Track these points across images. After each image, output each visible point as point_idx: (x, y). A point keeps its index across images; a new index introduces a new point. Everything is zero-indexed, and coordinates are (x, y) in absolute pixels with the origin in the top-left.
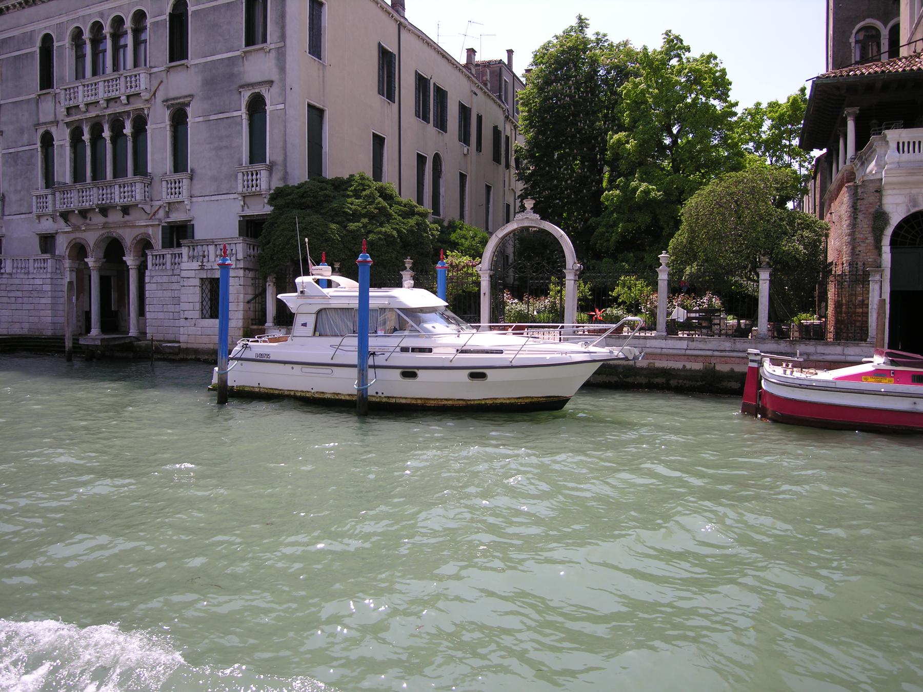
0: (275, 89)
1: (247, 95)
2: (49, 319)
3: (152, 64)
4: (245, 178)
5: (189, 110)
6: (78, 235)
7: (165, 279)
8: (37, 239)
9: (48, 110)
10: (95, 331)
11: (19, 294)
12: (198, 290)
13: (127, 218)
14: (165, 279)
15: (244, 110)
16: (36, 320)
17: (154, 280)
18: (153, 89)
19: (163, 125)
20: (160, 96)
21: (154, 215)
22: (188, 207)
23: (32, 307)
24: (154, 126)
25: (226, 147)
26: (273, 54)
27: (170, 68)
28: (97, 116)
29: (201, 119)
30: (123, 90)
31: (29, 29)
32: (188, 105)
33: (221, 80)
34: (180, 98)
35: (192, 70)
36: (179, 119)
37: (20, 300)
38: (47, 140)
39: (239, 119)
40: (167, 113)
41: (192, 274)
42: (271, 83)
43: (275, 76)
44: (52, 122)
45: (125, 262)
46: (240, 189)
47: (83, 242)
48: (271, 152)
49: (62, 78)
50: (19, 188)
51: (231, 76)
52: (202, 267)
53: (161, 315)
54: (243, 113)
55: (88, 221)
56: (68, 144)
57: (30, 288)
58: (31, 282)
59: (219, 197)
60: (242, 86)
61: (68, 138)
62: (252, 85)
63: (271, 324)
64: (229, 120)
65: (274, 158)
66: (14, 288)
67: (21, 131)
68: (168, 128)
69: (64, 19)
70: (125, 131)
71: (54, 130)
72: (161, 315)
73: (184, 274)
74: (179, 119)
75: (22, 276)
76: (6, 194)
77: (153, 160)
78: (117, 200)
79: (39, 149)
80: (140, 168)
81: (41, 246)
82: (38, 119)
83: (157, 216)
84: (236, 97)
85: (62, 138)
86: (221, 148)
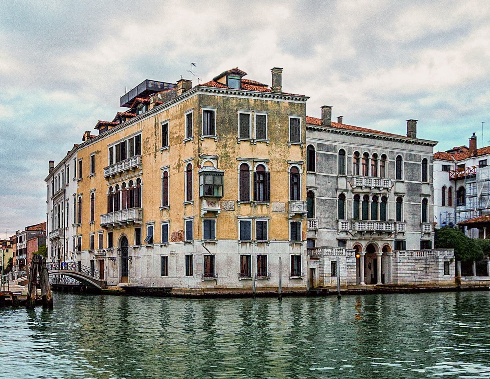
1: (422, 198)
9: (342, 183)
10: (363, 283)
14: (406, 261)
16: (350, 278)
17: (401, 262)
19: (394, 202)
25: (416, 215)
26: (430, 186)
29: (408, 203)
31: (334, 144)
33: (413, 189)
35: (404, 184)
36: (399, 201)
40: (396, 197)
42: (429, 196)
43: (431, 194)
44: (344, 190)
48: (428, 219)
50: (327, 216)
53: (404, 275)
54: (421, 203)
69: (352, 146)
71: (346, 193)
74: (399, 201)
80: (383, 217)
82: (338, 187)
85: (349, 197)
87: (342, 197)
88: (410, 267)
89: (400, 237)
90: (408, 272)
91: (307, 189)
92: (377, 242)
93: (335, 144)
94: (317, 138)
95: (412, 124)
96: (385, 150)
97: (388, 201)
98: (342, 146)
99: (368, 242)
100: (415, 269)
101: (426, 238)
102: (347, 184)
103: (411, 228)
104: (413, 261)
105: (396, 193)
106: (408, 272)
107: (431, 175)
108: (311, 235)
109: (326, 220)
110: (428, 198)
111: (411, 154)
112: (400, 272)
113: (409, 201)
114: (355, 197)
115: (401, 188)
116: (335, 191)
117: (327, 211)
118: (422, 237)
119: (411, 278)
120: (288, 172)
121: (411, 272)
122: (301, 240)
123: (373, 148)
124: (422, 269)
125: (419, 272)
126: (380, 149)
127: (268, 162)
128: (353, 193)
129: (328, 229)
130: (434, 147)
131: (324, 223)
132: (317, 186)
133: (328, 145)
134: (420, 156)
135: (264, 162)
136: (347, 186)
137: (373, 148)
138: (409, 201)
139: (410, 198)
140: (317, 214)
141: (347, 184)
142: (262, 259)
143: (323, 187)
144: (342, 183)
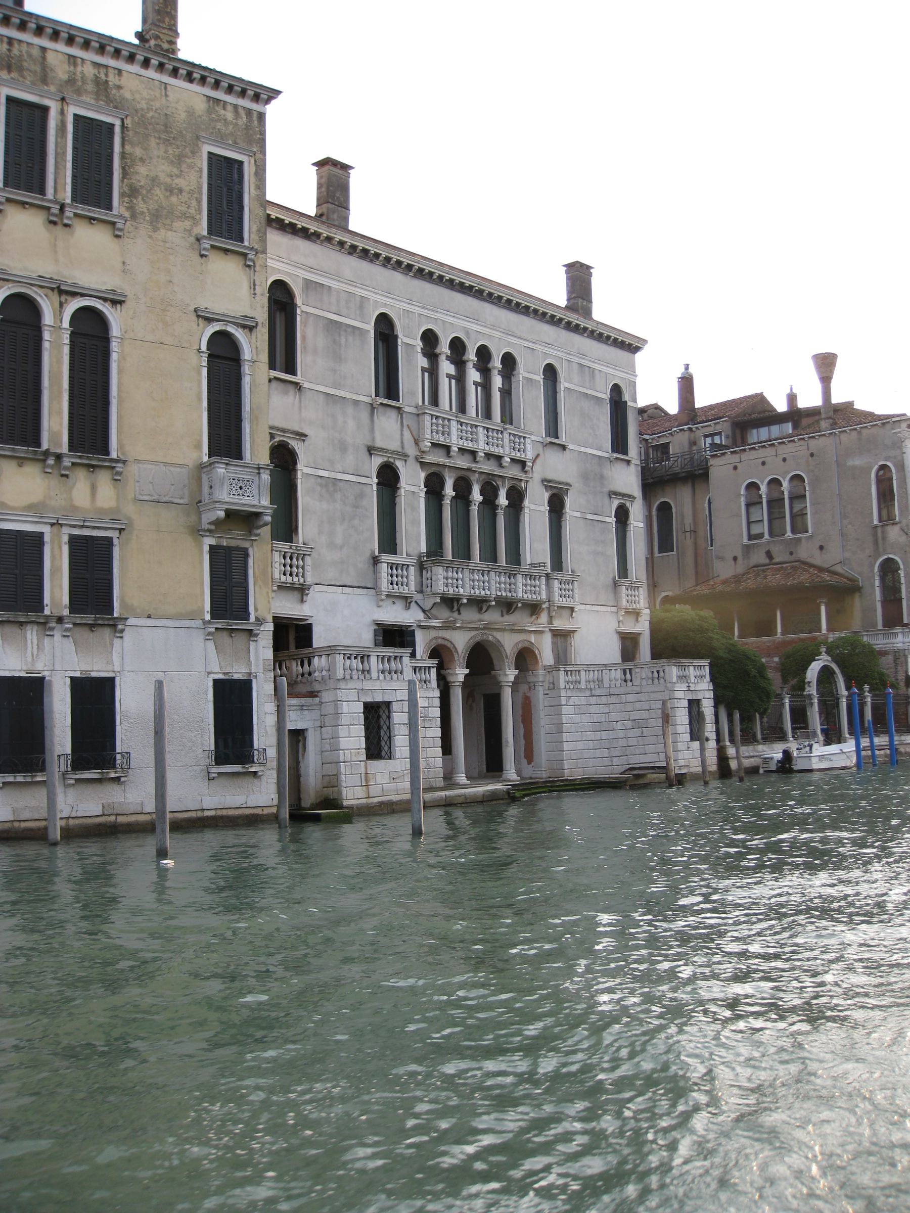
1: (615, 503)
10: (462, 779)
14: (583, 701)
24: (533, 507)
31: (359, 292)
34: (559, 483)
36: (556, 505)
40: (546, 495)
50: (339, 540)
53: (580, 745)
60: (616, 494)
67: (343, 448)
71: (399, 464)
72: (580, 745)
74: (556, 505)
80: (515, 555)
82: (373, 439)
84: (607, 500)
85: (412, 482)
87: (388, 478)
88: (596, 718)
90: (591, 736)
91: (272, 436)
92: (498, 635)
93: (364, 293)
95: (579, 277)
97: (526, 503)
101: (630, 627)
102: (402, 435)
104: (604, 700)
105: (547, 483)
106: (591, 736)
108: (288, 608)
120: (199, 351)
122: (252, 619)
123: (479, 328)
124: (629, 724)
125: (621, 734)
126: (497, 334)
127: (121, 302)
128: (423, 464)
130: (638, 355)
135: (105, 300)
141: (402, 435)
142: (95, 698)
144: (389, 431)
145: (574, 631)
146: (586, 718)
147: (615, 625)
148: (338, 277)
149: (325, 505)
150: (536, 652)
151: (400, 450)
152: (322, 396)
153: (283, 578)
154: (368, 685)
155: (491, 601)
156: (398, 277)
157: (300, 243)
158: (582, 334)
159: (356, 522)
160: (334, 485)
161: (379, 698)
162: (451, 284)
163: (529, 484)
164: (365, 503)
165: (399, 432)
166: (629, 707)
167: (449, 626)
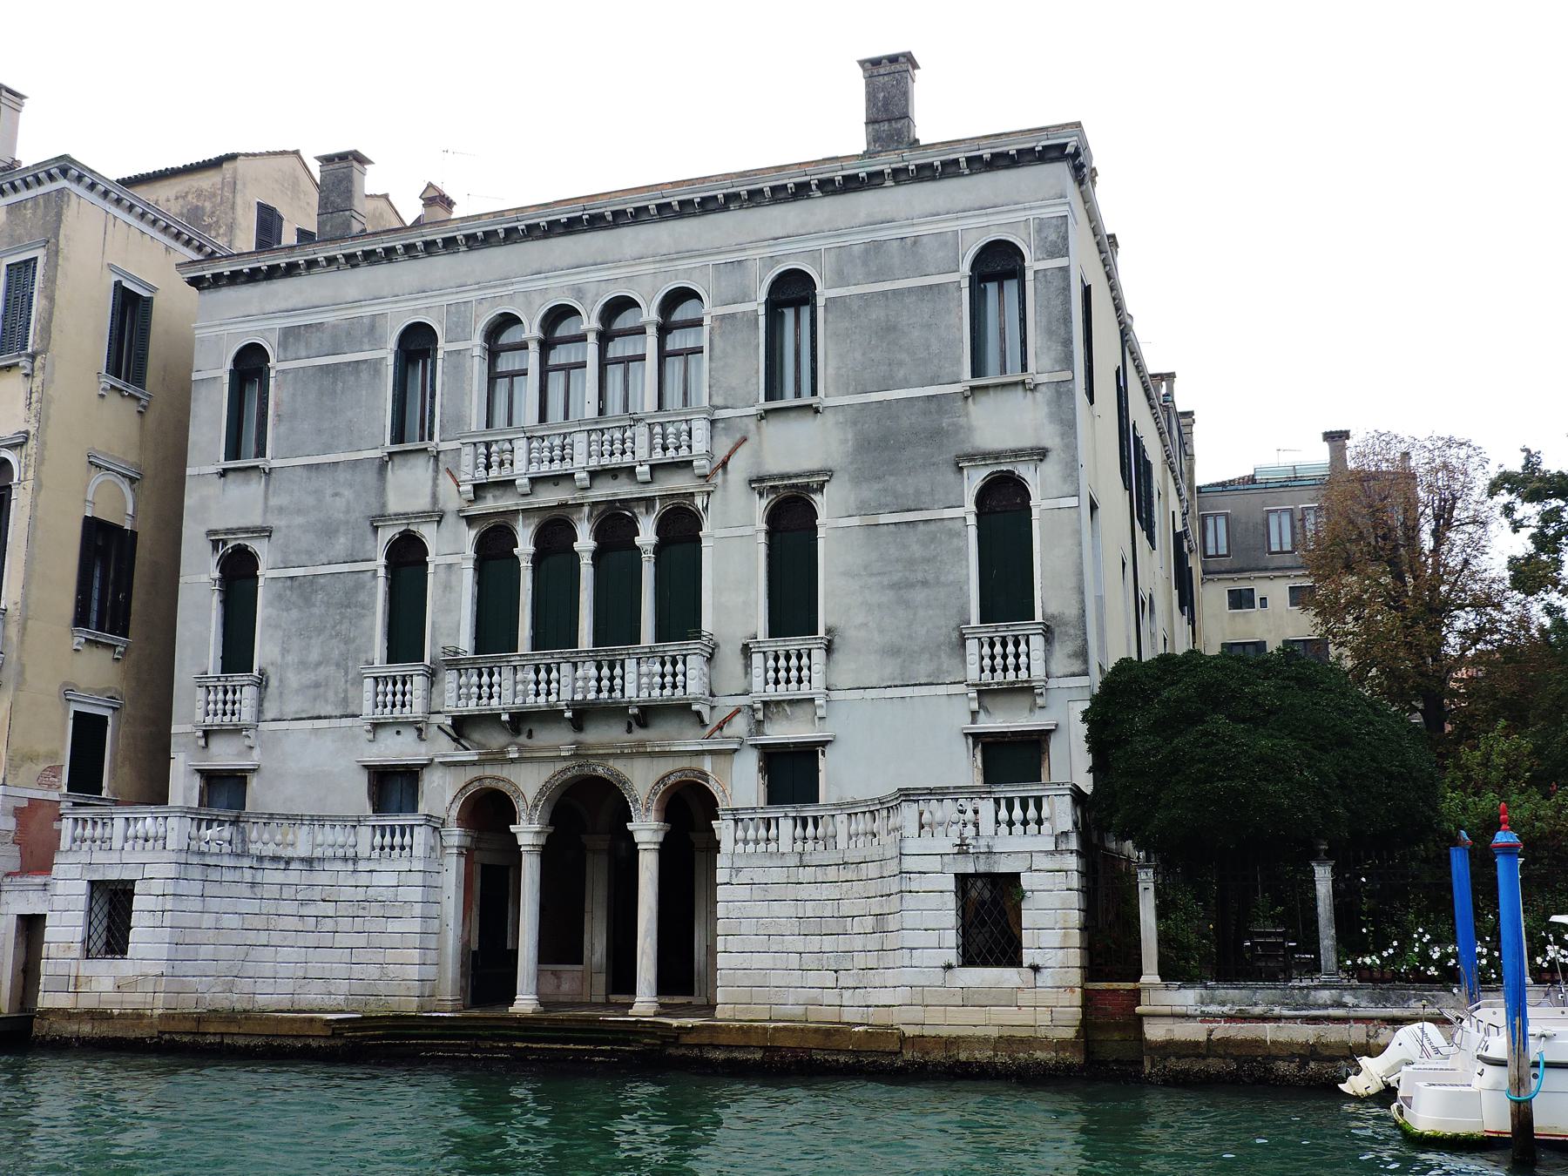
0: (1050, 467)
1: (975, 479)
2: (414, 972)
3: (718, 401)
4: (986, 650)
5: (821, 502)
6: (489, 771)
7: (777, 875)
8: (362, 783)
9: (410, 488)
11: (329, 909)
12: (951, 901)
13: (639, 734)
14: (777, 875)
15: (970, 506)
16: (374, 972)
17: (744, 877)
18: (720, 455)
19: (749, 531)
20: (740, 468)
21: (720, 727)
22: (820, 713)
23: (361, 940)
27: (766, 411)
28: (563, 505)
29: (856, 521)
30: (642, 453)
32: (821, 486)
34: (797, 476)
35: (828, 419)
36: (791, 517)
37: (328, 924)
38: (407, 558)
39: (959, 524)
40: (761, 506)
41: (935, 864)
42: (1041, 454)
43: (1049, 437)
45: (630, 834)
46: (973, 674)
47: (501, 786)
48: (1047, 596)
49: (459, 419)
50: (314, 656)
51: (936, 435)
52: (962, 849)
53: (765, 960)
55: (523, 739)
56: (469, 566)
57: (360, 894)
58: (364, 879)
59: (908, 692)
60: (971, 457)
61: (470, 552)
62: (997, 456)
63: (1157, 979)
64: (932, 527)
65: (1053, 609)
66: (317, 894)
67: (328, 530)
68: (762, 538)
69: (473, 296)
70: (638, 541)
71: (428, 533)
72: (765, 960)
73: (909, 863)
74: (791, 517)
75: (339, 866)
76: (270, 671)
77: (717, 608)
78: (630, 691)
79: (382, 572)
81: (371, 795)
82: (384, 505)
83: (727, 731)
84: (951, 476)
86: (911, 586)
89: (782, 732)
90: (798, 943)
92: (619, 766)
93: (376, 310)
94: (284, 306)
96: (682, 265)
98: (415, 311)
99: (563, 771)
100: (838, 925)
101: (1006, 720)
103: (891, 668)
104: (832, 873)
105: (757, 483)
106: (798, 943)
107: (1050, 333)
108: (224, 755)
109: (309, 677)
110: (1025, 471)
111: (876, 247)
112: (734, 943)
113: (863, 509)
114: (482, 545)
115: (792, 448)
116: (369, 529)
117: (320, 631)
118: (974, 714)
119: (812, 978)
121: (814, 943)
123: (605, 275)
125: (858, 942)
128: (470, 520)
129: (319, 718)
131: (303, 689)
132: (273, 521)
133: (334, 326)
134: (951, 242)
136: (434, 497)
137: (605, 275)
138: (863, 509)
139: (868, 492)
140: (264, 650)
143: (300, 520)
144: (410, 488)
145: (824, 744)
146: (787, 909)
147: (965, 723)
148: (336, 305)
149: (295, 613)
150: (713, 787)
151: (428, 507)
152: (299, 471)
153: (209, 720)
154: (99, 857)
155: (562, 711)
156: (441, 265)
157: (281, 286)
158: (880, 186)
159: (344, 627)
160: (312, 583)
161: (113, 875)
162: (533, 232)
163: (715, 500)
164: (363, 597)
165: (430, 483)
166: (873, 888)
167: (499, 758)
